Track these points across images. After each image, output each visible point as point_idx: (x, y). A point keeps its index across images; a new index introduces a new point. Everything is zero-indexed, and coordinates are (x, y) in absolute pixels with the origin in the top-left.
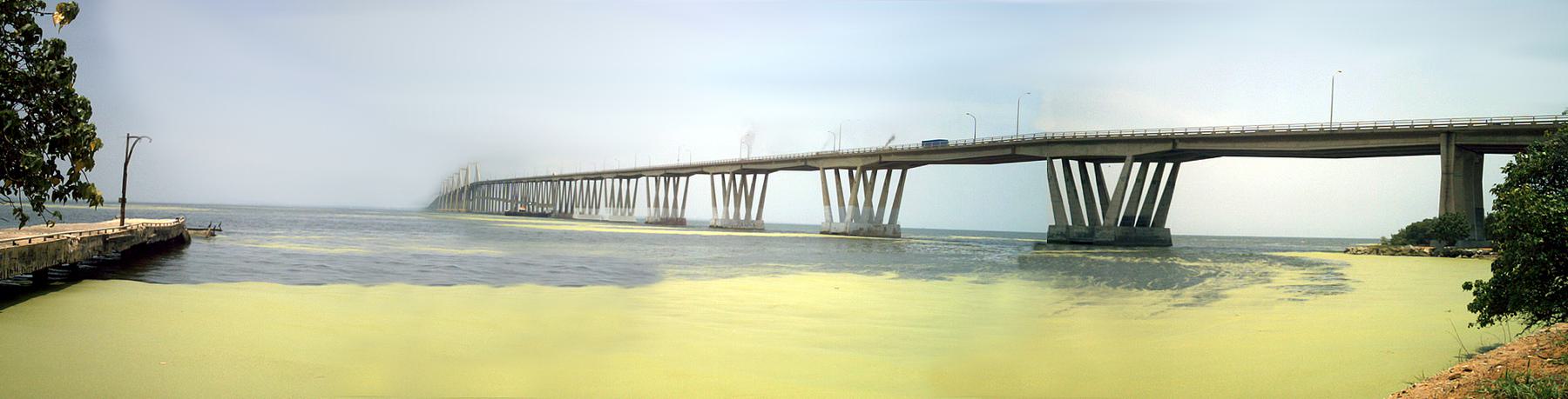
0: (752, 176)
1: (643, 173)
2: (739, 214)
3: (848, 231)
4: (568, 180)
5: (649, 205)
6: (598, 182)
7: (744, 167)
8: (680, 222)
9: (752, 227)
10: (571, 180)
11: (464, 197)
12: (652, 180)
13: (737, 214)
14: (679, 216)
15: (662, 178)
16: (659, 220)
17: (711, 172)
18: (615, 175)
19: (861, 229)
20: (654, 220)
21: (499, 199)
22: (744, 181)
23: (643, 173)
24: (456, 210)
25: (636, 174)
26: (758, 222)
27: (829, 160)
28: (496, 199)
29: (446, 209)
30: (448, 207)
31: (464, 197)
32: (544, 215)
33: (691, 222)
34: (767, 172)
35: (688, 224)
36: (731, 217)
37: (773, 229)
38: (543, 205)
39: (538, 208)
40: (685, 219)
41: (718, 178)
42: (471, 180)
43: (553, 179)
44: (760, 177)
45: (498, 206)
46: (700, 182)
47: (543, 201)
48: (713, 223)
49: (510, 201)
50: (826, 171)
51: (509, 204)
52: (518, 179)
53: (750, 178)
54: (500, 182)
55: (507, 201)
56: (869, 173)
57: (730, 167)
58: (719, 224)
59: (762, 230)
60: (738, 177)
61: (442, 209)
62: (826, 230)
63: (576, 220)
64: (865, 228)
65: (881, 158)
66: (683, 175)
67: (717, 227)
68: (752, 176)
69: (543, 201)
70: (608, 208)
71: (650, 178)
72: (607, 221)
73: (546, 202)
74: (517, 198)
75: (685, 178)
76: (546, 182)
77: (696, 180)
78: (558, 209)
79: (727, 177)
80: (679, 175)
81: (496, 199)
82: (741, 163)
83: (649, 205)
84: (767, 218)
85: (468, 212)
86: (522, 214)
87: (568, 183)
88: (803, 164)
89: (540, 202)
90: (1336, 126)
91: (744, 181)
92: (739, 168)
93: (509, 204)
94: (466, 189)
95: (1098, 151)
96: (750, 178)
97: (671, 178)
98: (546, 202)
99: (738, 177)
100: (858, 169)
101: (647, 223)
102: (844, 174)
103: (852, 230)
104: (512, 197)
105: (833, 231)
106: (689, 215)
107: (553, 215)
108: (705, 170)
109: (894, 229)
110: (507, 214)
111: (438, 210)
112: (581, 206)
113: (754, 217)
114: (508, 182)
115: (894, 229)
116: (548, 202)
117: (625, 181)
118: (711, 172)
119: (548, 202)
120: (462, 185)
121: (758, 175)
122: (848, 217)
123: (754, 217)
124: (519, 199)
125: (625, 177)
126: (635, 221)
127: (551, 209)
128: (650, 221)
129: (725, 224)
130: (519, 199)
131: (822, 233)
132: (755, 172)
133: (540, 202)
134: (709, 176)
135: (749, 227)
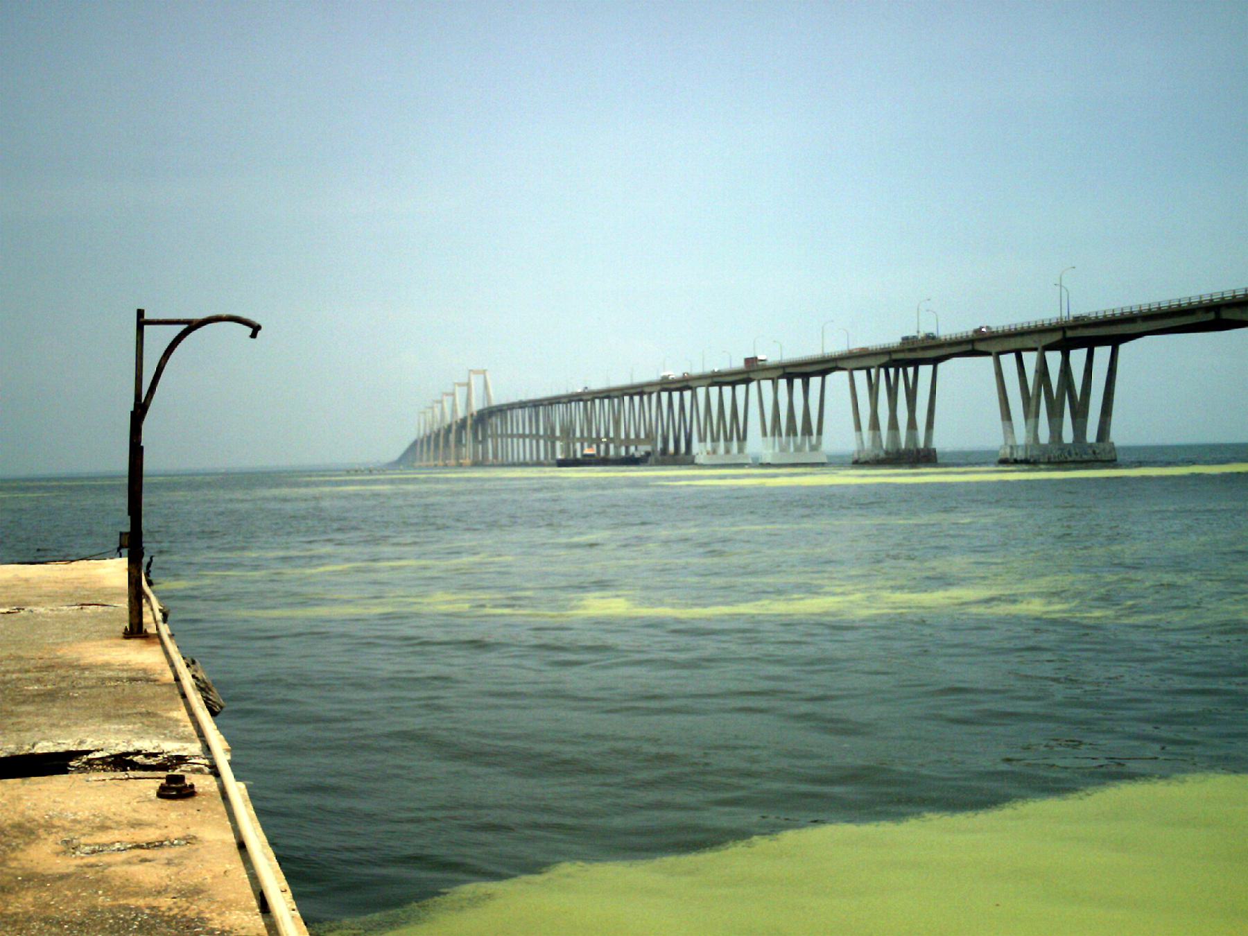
0: (1084, 351)
1: (840, 364)
4: (676, 389)
5: (858, 427)
7: (1070, 334)
8: (924, 457)
10: (641, 394)
11: (452, 437)
14: (921, 444)
15: (882, 371)
16: (882, 455)
17: (994, 351)
18: (709, 381)
20: (872, 456)
21: (523, 436)
23: (840, 364)
25: (824, 366)
27: (997, 340)
28: (523, 436)
29: (440, 463)
31: (452, 437)
32: (631, 461)
33: (944, 454)
34: (1115, 342)
35: (939, 461)
37: (1166, 458)
38: (627, 442)
39: (617, 448)
40: (934, 450)
42: (477, 405)
43: (612, 394)
44: (1102, 354)
45: (522, 449)
48: (1006, 453)
50: (1002, 357)
52: (1081, 323)
54: (522, 405)
55: (537, 437)
57: (1036, 337)
58: (1020, 455)
59: (1111, 463)
61: (424, 463)
63: (702, 466)
65: (1064, 332)
66: (926, 361)
68: (1084, 351)
69: (627, 435)
70: (769, 438)
71: (856, 373)
72: (768, 465)
73: (632, 436)
74: (553, 430)
75: (930, 368)
76: (790, 379)
77: (838, 379)
78: (659, 445)
80: (916, 363)
82: (1061, 328)
83: (858, 427)
84: (1119, 435)
85: (477, 464)
86: (587, 461)
87: (676, 395)
88: (1211, 316)
92: (1057, 337)
94: (469, 422)
96: (1078, 357)
98: (632, 436)
100: (1040, 349)
101: (858, 463)
104: (545, 430)
106: (942, 441)
107: (651, 459)
108: (981, 347)
110: (562, 463)
111: (417, 464)
113: (1091, 436)
114: (536, 404)
116: (637, 435)
117: (798, 383)
118: (994, 351)
119: (637, 435)
120: (461, 414)
121: (1097, 350)
123: (1091, 436)
124: (558, 433)
125: (727, 384)
126: (824, 460)
127: (643, 449)
128: (863, 457)
130: (558, 433)
132: (1090, 344)
133: (623, 436)
134: (845, 374)
135: (1086, 457)
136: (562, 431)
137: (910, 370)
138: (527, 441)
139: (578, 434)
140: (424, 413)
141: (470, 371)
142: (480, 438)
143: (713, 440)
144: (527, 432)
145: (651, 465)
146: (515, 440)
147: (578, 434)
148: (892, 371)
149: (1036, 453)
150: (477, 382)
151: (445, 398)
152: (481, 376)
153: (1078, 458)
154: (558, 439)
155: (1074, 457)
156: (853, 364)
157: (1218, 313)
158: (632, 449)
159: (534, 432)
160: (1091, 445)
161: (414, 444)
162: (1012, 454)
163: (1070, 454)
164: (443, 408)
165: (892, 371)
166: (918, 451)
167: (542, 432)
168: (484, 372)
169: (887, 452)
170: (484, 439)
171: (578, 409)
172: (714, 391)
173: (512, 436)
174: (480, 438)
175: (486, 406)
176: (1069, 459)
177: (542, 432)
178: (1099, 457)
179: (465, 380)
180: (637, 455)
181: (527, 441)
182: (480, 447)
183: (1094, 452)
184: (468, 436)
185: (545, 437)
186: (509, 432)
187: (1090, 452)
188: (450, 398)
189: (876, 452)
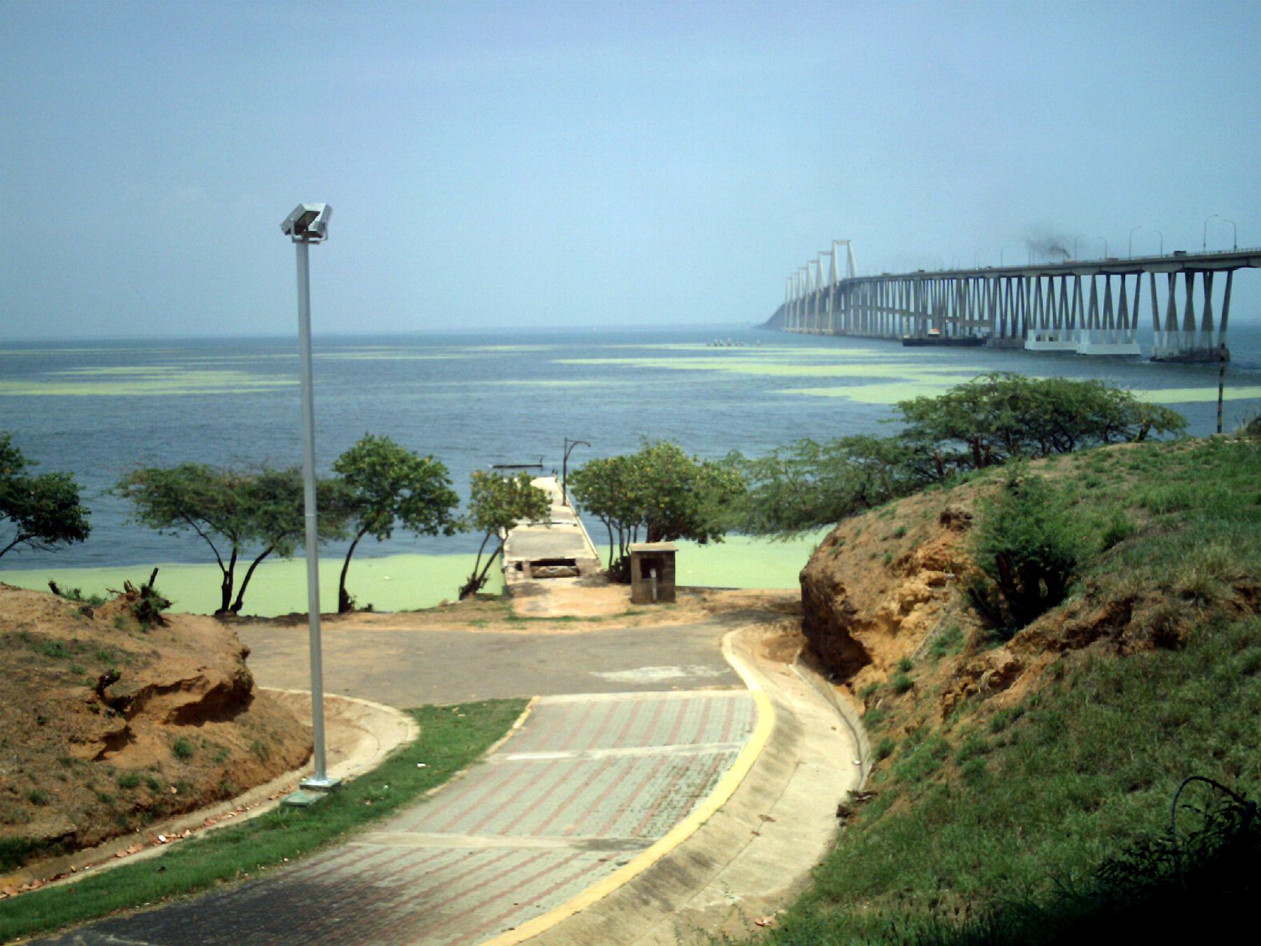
11: (829, 305)
16: (1176, 353)
21: (893, 310)
25: (1136, 267)
30: (801, 325)
42: (841, 274)
73: (976, 317)
74: (925, 308)
89: (967, 318)
94: (832, 291)
98: (976, 317)
114: (907, 278)
116: (981, 316)
119: (981, 316)
120: (825, 282)
124: (930, 311)
127: (986, 330)
130: (930, 311)
133: (967, 318)
138: (897, 316)
140: (791, 278)
142: (843, 308)
144: (897, 307)
145: (989, 348)
146: (885, 314)
150: (840, 252)
152: (845, 247)
154: (929, 316)
158: (976, 329)
159: (904, 307)
161: (782, 310)
169: (1181, 351)
170: (846, 311)
173: (881, 309)
174: (843, 308)
177: (912, 309)
179: (829, 249)
180: (979, 336)
182: (843, 316)
185: (916, 314)
186: (879, 304)
188: (815, 265)
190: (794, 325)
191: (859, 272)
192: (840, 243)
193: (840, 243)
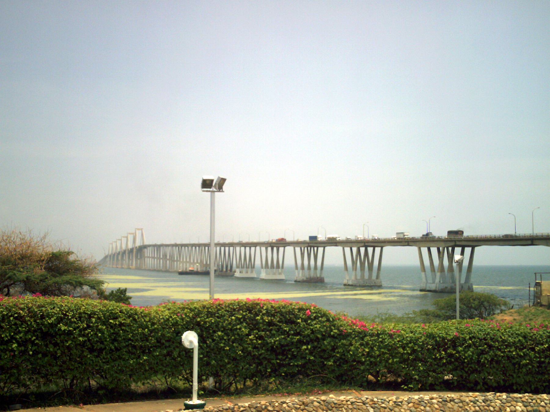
2: (364, 276)
3: (437, 289)
6: (231, 248)
9: (374, 284)
12: (298, 249)
13: (363, 276)
15: (306, 248)
16: (305, 279)
19: (446, 288)
22: (366, 251)
24: (115, 266)
26: (377, 280)
36: (359, 277)
41: (347, 250)
42: (138, 244)
46: (289, 250)
47: (194, 261)
49: (162, 259)
51: (161, 261)
53: (370, 250)
56: (450, 249)
58: (350, 283)
60: (362, 250)
62: (424, 288)
64: (449, 287)
67: (349, 285)
79: (355, 249)
81: (152, 257)
87: (227, 248)
89: (192, 261)
90: (535, 234)
91: (366, 251)
93: (161, 261)
94: (135, 250)
95: (376, 244)
97: (312, 248)
99: (362, 250)
102: (434, 250)
103: (440, 288)
105: (428, 289)
109: (469, 287)
112: (245, 266)
115: (469, 287)
122: (437, 280)
129: (361, 283)
131: (421, 290)
133: (205, 263)
136: (170, 256)
137: (316, 248)
139: (176, 259)
141: (136, 229)
142: (139, 257)
143: (247, 268)
147: (176, 259)
148: (309, 248)
149: (355, 282)
150: (138, 234)
151: (123, 238)
152: (140, 231)
153: (369, 285)
155: (368, 284)
156: (376, 244)
157: (455, 242)
160: (374, 280)
161: (106, 257)
162: (348, 282)
163: (367, 283)
164: (116, 245)
165: (309, 248)
166: (318, 278)
167: (161, 257)
168: (142, 229)
169: (307, 278)
171: (176, 249)
172: (243, 248)
173: (149, 257)
174: (139, 257)
175: (142, 244)
176: (366, 285)
177: (161, 257)
178: (376, 284)
181: (156, 260)
182: (139, 261)
183: (375, 283)
184: (126, 257)
187: (373, 282)
189: (303, 278)
190: (110, 264)
191: (146, 243)
192: (138, 229)
193: (138, 229)
